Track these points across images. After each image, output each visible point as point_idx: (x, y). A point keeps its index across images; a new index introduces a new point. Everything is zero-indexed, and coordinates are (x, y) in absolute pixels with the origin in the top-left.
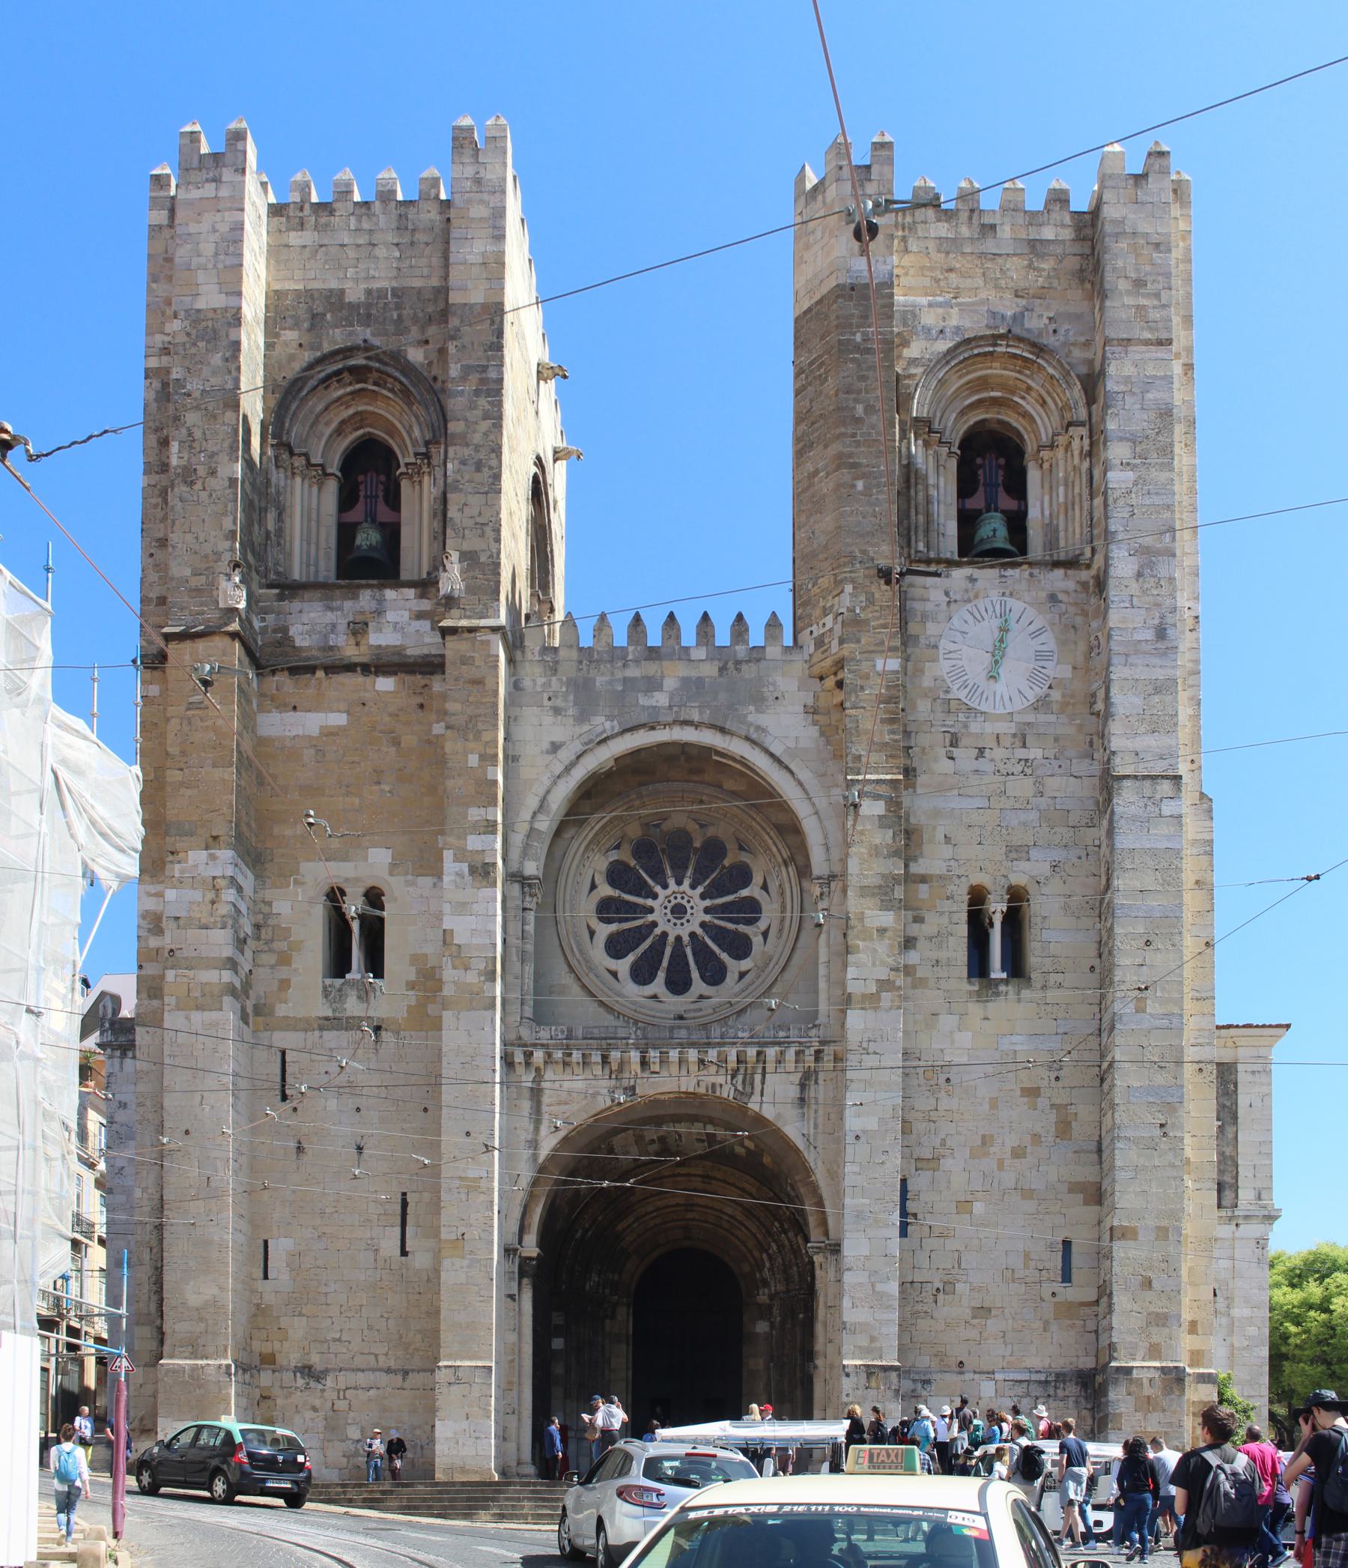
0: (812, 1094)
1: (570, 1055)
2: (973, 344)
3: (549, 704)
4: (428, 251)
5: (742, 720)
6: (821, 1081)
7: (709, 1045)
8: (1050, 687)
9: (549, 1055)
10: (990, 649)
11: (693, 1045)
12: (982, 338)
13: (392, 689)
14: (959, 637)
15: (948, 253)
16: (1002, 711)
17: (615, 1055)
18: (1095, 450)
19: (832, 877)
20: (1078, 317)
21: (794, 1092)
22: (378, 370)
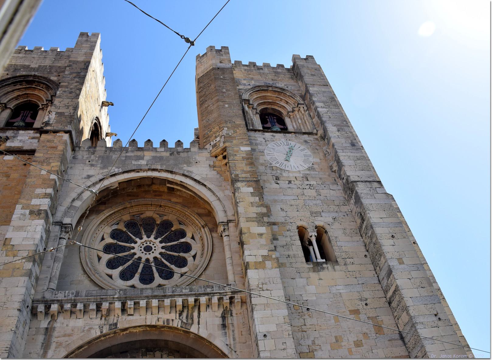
0: (230, 321)
1: (75, 306)
2: (260, 87)
3: (89, 163)
4: (65, 60)
5: (181, 169)
6: (234, 314)
7: (165, 296)
8: (313, 164)
9: (62, 307)
10: (286, 153)
11: (155, 297)
12: (263, 86)
13: (12, 159)
14: (271, 150)
15: (248, 72)
16: (295, 170)
17: (105, 305)
18: (309, 109)
19: (229, 221)
20: (294, 85)
21: (219, 321)
22: (37, 82)
